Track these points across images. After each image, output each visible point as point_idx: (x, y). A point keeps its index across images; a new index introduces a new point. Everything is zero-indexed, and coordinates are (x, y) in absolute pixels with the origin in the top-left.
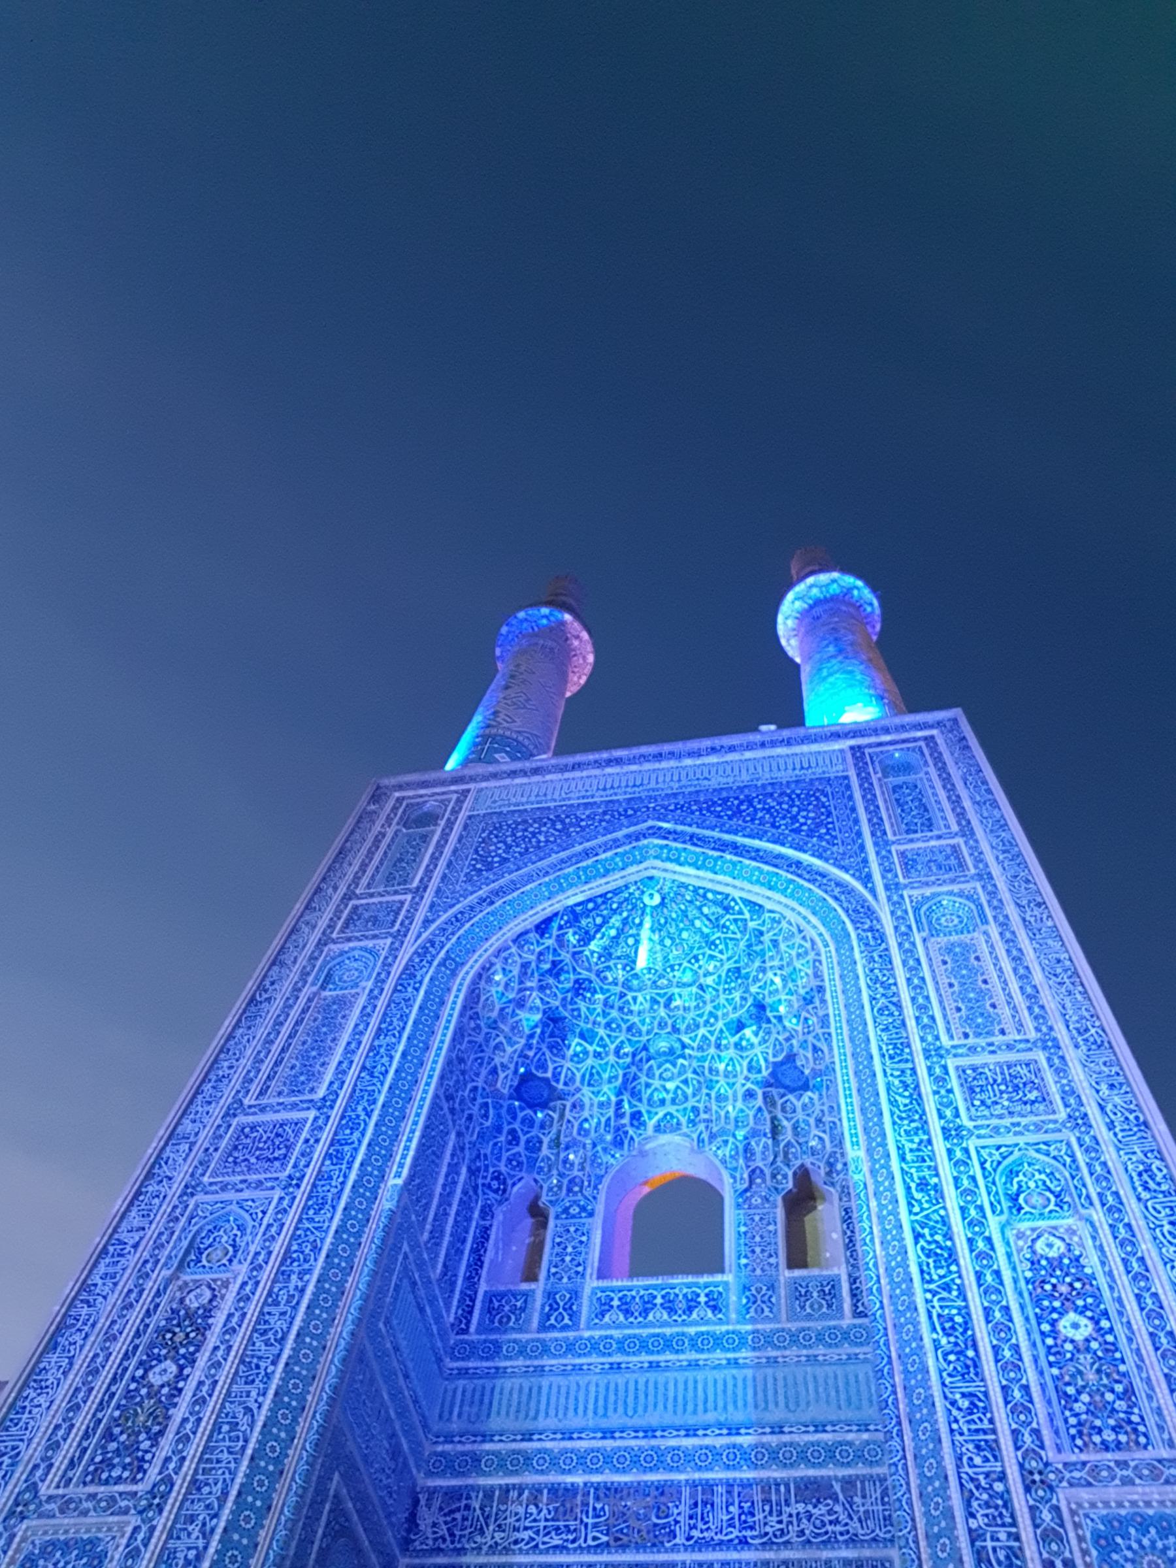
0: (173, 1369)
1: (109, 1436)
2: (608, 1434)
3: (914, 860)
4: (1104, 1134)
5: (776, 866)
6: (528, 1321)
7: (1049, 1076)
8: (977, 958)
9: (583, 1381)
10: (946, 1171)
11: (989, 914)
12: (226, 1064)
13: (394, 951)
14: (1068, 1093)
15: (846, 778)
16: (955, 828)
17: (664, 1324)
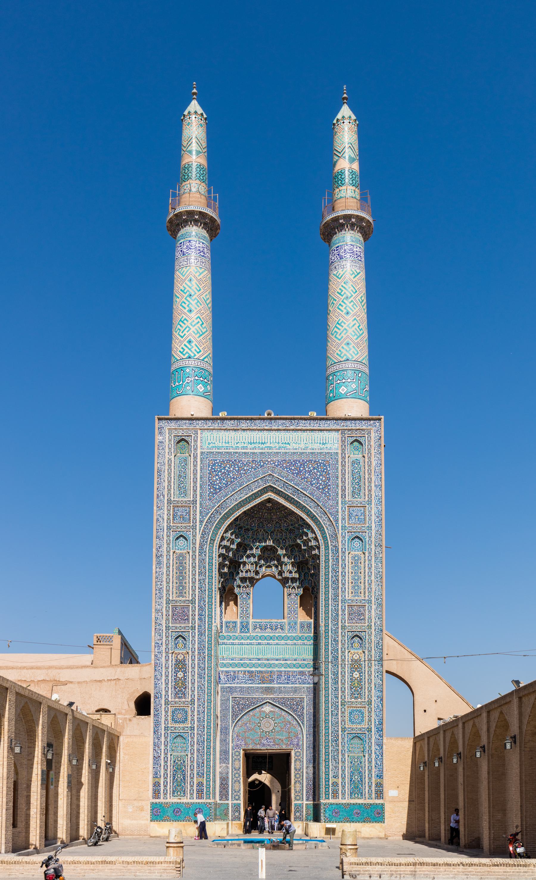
0: (182, 674)
1: (175, 688)
2: (259, 659)
3: (352, 514)
4: (373, 632)
5: (310, 507)
6: (237, 630)
7: (367, 613)
8: (361, 563)
9: (252, 646)
10: (340, 638)
11: (367, 547)
12: (159, 583)
13: (194, 536)
14: (370, 618)
15: (337, 453)
16: (367, 499)
17: (270, 633)
